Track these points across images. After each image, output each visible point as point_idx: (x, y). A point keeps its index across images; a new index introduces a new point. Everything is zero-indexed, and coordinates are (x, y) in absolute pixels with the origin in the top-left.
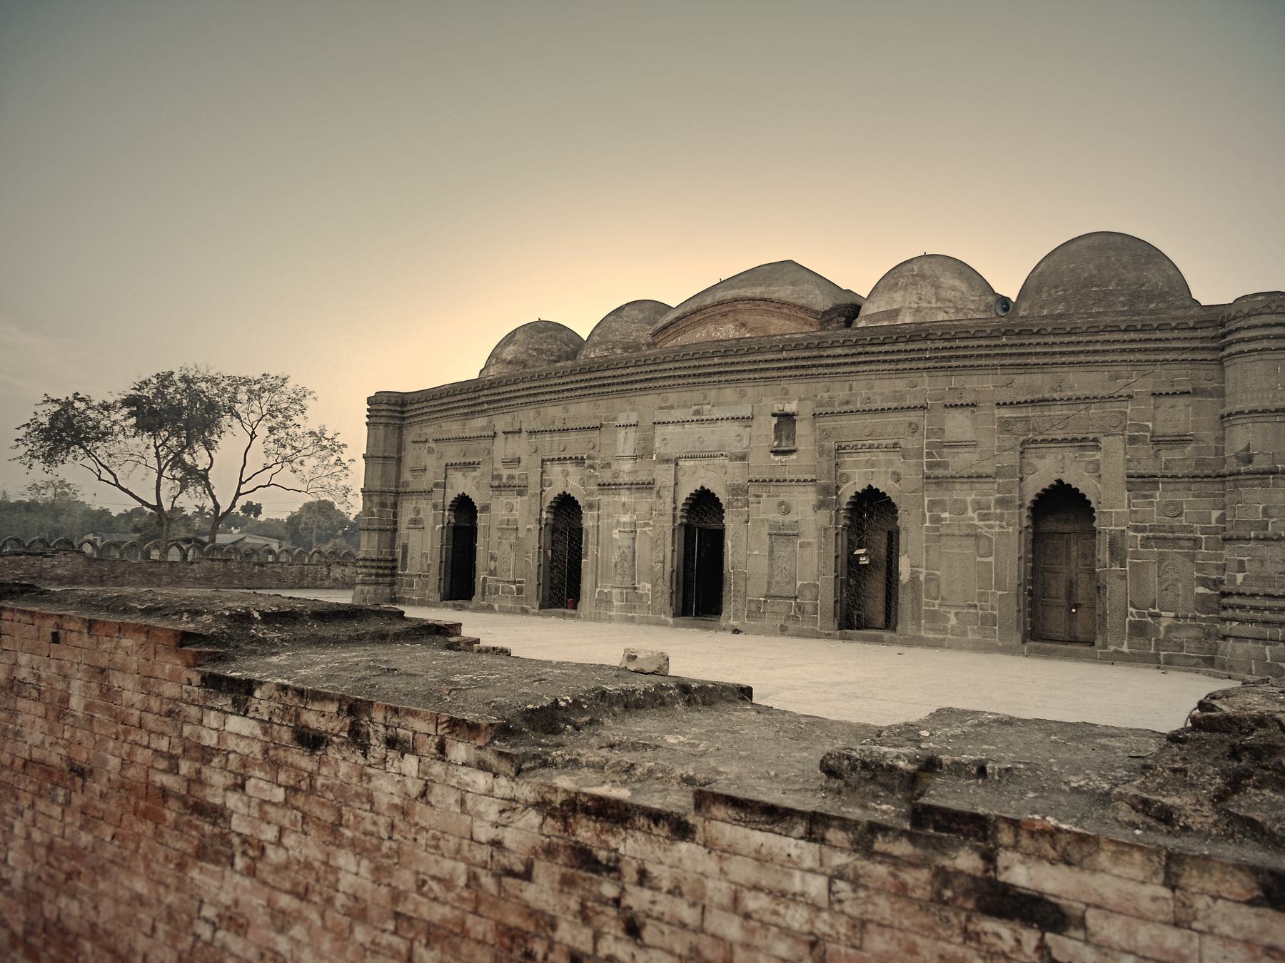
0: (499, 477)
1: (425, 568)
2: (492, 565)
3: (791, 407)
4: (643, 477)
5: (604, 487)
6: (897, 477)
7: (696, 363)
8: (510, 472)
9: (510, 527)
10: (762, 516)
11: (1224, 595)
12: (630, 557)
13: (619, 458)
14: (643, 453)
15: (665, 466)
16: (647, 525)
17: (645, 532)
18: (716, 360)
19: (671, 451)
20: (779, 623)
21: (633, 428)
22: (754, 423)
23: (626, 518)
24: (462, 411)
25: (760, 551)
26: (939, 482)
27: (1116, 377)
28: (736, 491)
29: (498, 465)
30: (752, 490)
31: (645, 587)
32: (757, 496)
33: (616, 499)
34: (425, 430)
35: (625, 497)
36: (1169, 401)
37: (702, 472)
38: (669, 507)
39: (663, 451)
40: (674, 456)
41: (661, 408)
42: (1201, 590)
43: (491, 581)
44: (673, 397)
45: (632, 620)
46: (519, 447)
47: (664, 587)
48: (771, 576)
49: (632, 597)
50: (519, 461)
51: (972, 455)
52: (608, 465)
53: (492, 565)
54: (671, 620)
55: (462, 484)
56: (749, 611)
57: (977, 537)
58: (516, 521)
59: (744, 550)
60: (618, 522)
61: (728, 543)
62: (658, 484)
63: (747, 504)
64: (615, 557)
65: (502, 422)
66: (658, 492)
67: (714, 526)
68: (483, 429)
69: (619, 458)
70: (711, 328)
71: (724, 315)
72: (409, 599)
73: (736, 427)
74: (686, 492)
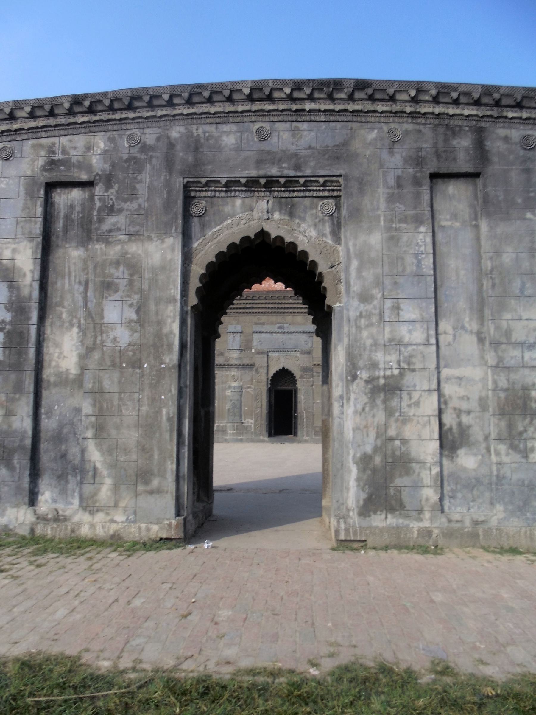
4: (246, 361)
7: (280, 301)
12: (238, 406)
13: (229, 350)
14: (246, 347)
15: (261, 356)
16: (249, 388)
17: (248, 392)
19: (265, 347)
23: (235, 384)
30: (315, 369)
31: (250, 422)
33: (228, 373)
35: (234, 372)
37: (282, 359)
38: (264, 378)
39: (259, 347)
40: (266, 350)
41: (256, 324)
44: (264, 318)
45: (241, 441)
47: (264, 423)
54: (266, 439)
56: (316, 432)
60: (230, 387)
61: (301, 397)
62: (257, 365)
66: (257, 370)
67: (293, 388)
69: (229, 350)
74: (273, 371)
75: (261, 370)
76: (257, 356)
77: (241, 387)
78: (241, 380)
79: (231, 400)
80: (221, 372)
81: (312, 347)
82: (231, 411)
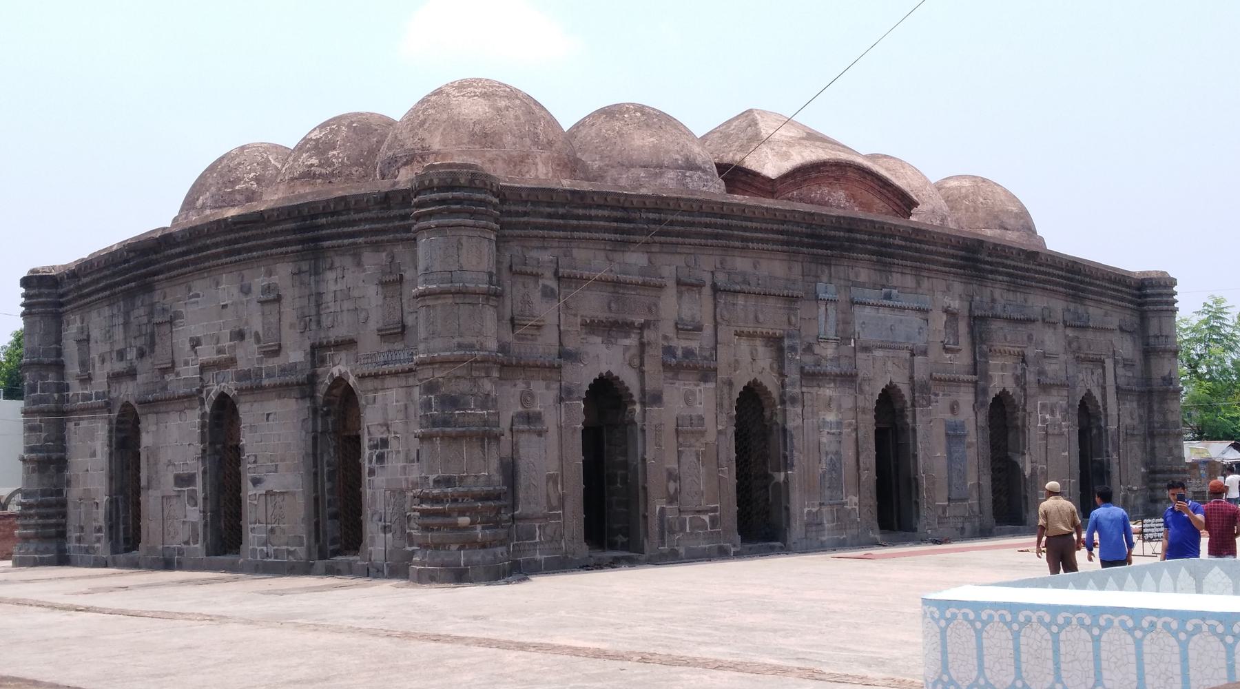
0: (669, 351)
1: (555, 502)
2: (672, 486)
3: (955, 304)
4: (845, 366)
6: (1020, 380)
8: (684, 343)
9: (686, 429)
10: (941, 416)
11: (1153, 472)
18: (898, 242)
20: (960, 525)
21: (831, 307)
22: (931, 316)
23: (831, 417)
24: (612, 236)
25: (940, 453)
26: (1045, 388)
27: (1106, 315)
28: (925, 388)
29: (671, 332)
30: (933, 389)
31: (852, 501)
32: (936, 395)
34: (534, 254)
35: (828, 391)
36: (1127, 337)
37: (889, 363)
41: (855, 285)
42: (1143, 470)
43: (672, 512)
44: (864, 274)
46: (699, 308)
48: (950, 479)
49: (842, 517)
50: (698, 328)
51: (1057, 367)
52: (809, 349)
53: (672, 486)
54: (878, 537)
55: (607, 358)
57: (1062, 434)
58: (701, 418)
59: (931, 453)
60: (824, 422)
62: (861, 375)
63: (929, 404)
65: (669, 266)
68: (642, 272)
70: (826, 190)
72: (528, 562)
73: (916, 320)
75: (866, 388)
77: (839, 424)
78: (839, 407)
79: (827, 454)
80: (810, 389)
81: (927, 342)
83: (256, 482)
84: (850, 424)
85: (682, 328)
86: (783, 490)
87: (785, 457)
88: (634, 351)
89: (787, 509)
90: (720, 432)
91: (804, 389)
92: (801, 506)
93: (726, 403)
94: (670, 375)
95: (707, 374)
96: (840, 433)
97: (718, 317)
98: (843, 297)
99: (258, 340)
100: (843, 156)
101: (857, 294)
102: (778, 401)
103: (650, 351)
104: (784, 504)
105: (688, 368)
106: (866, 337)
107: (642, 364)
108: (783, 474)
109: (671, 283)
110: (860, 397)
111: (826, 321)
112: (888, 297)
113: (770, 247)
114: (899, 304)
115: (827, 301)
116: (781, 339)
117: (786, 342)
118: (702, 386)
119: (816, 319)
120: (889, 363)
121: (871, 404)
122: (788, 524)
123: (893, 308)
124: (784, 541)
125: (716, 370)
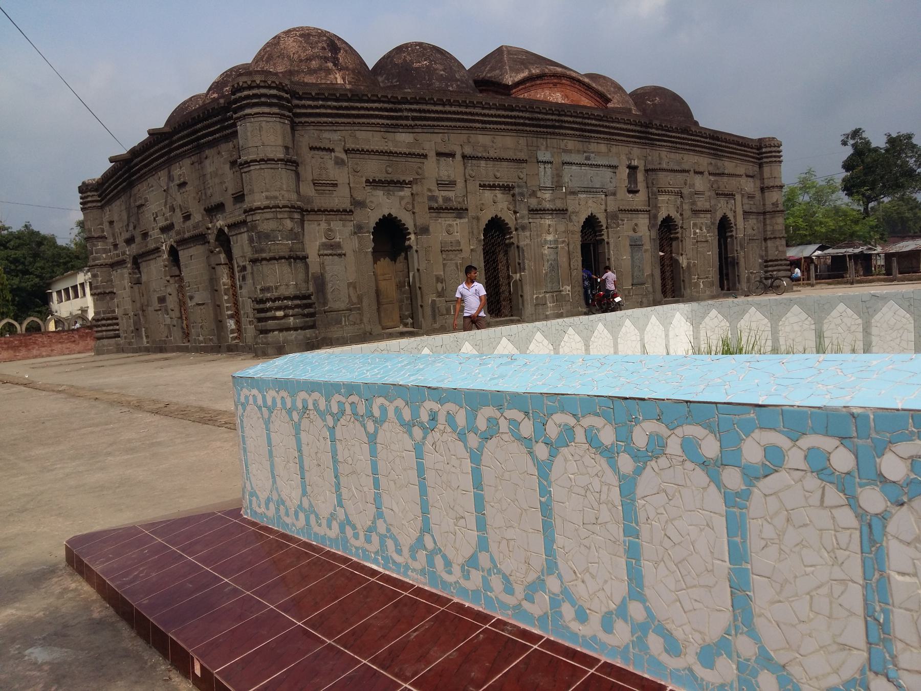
0: (433, 198)
4: (559, 205)
5: (534, 211)
13: (542, 189)
15: (572, 197)
16: (563, 242)
18: (593, 122)
21: (550, 166)
23: (550, 238)
29: (434, 187)
35: (548, 221)
41: (566, 151)
44: (570, 144)
46: (451, 169)
49: (559, 298)
52: (533, 194)
58: (458, 243)
62: (570, 209)
64: (545, 268)
69: (542, 189)
70: (547, 92)
71: (555, 85)
75: (574, 218)
76: (568, 197)
77: (556, 241)
78: (556, 231)
82: (549, 275)
83: (191, 298)
84: (563, 242)
85: (441, 184)
86: (519, 284)
87: (519, 264)
88: (409, 199)
89: (522, 296)
90: (472, 250)
91: (531, 220)
92: (530, 294)
93: (475, 232)
94: (434, 215)
95: (460, 212)
96: (557, 248)
97: (467, 175)
98: (557, 160)
99: (181, 210)
100: (559, 69)
101: (566, 158)
102: (513, 229)
103: (418, 199)
104: (520, 293)
105: (446, 209)
106: (575, 184)
107: (413, 207)
108: (518, 275)
109: (432, 154)
110: (570, 224)
111: (545, 176)
112: (588, 158)
113: (503, 127)
114: (595, 163)
115: (545, 163)
116: (513, 187)
117: (517, 190)
118: (458, 221)
119: (538, 174)
120: (590, 202)
121: (578, 228)
122: (523, 305)
123: (591, 165)
124: (520, 315)
125: (467, 210)
